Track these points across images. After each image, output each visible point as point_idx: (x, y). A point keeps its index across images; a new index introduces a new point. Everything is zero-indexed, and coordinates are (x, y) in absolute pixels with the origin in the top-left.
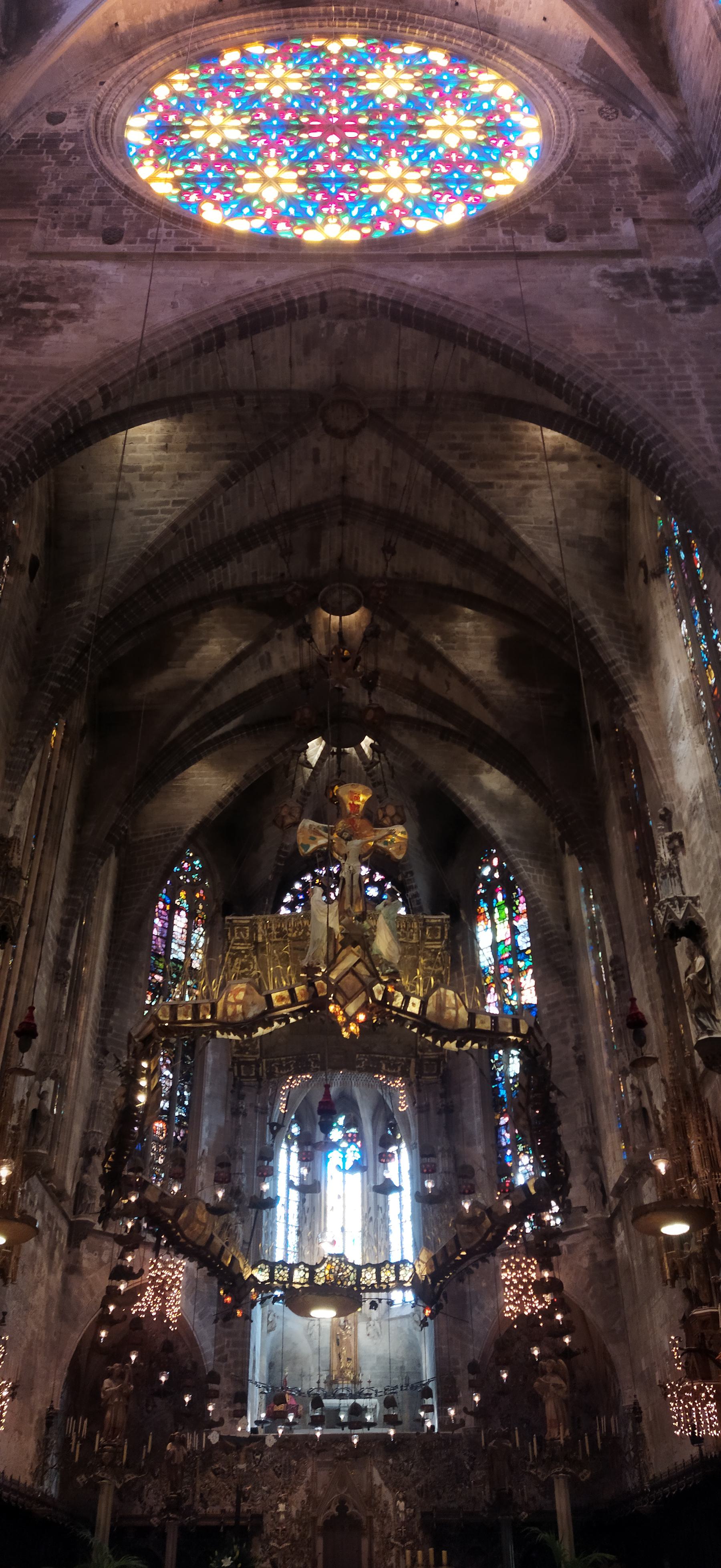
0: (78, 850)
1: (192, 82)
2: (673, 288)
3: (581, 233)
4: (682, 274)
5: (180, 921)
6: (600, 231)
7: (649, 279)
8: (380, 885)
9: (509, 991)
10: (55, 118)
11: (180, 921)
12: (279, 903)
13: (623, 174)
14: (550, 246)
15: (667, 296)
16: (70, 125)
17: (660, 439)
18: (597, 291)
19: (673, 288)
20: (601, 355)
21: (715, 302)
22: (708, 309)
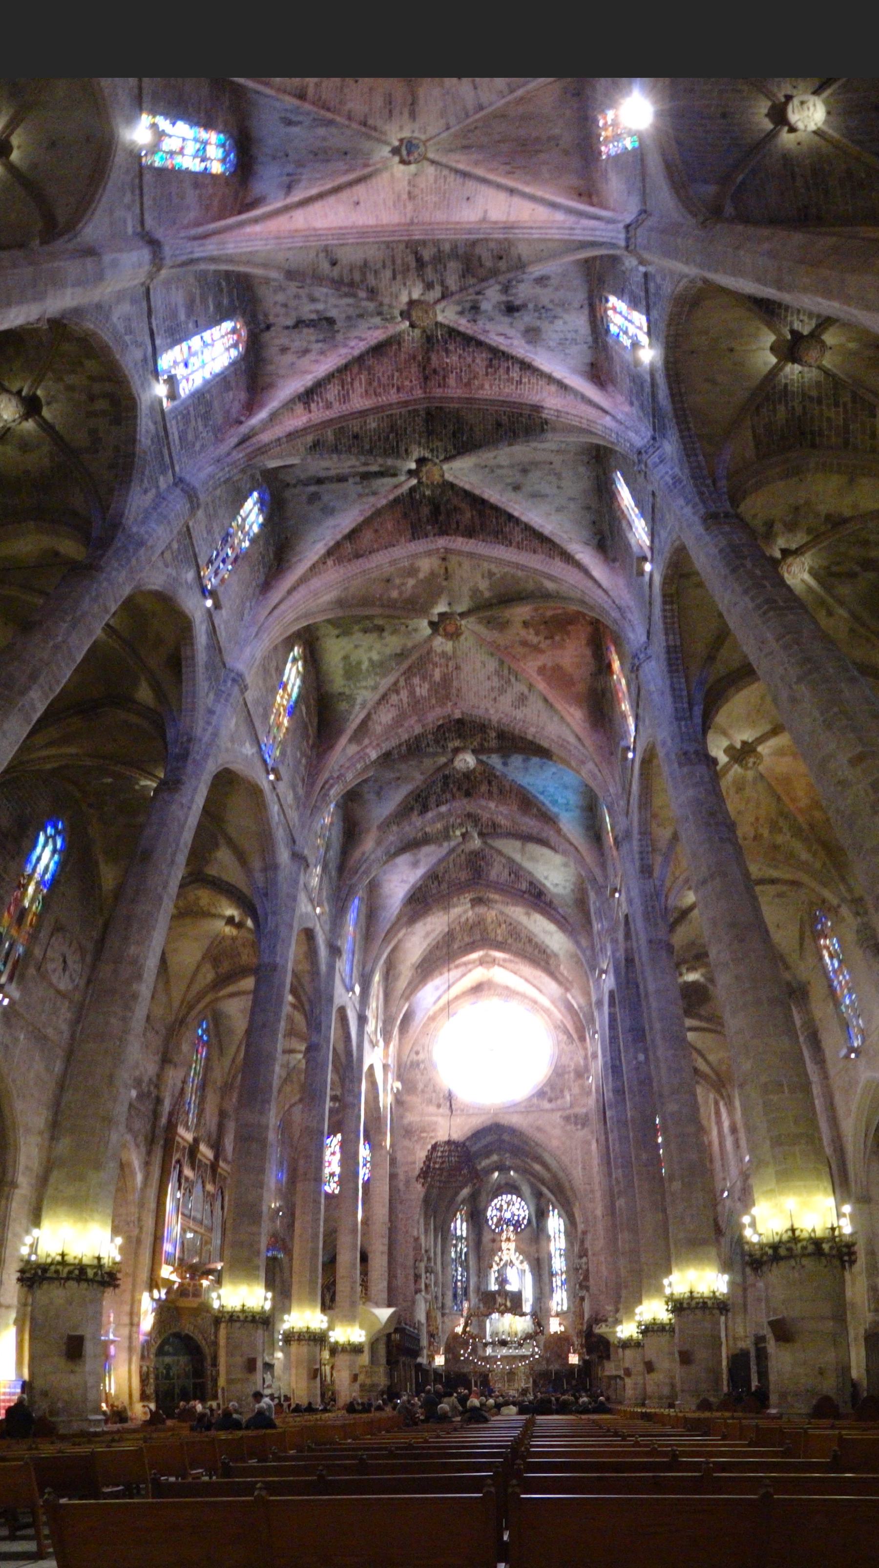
16: (421, 1056)
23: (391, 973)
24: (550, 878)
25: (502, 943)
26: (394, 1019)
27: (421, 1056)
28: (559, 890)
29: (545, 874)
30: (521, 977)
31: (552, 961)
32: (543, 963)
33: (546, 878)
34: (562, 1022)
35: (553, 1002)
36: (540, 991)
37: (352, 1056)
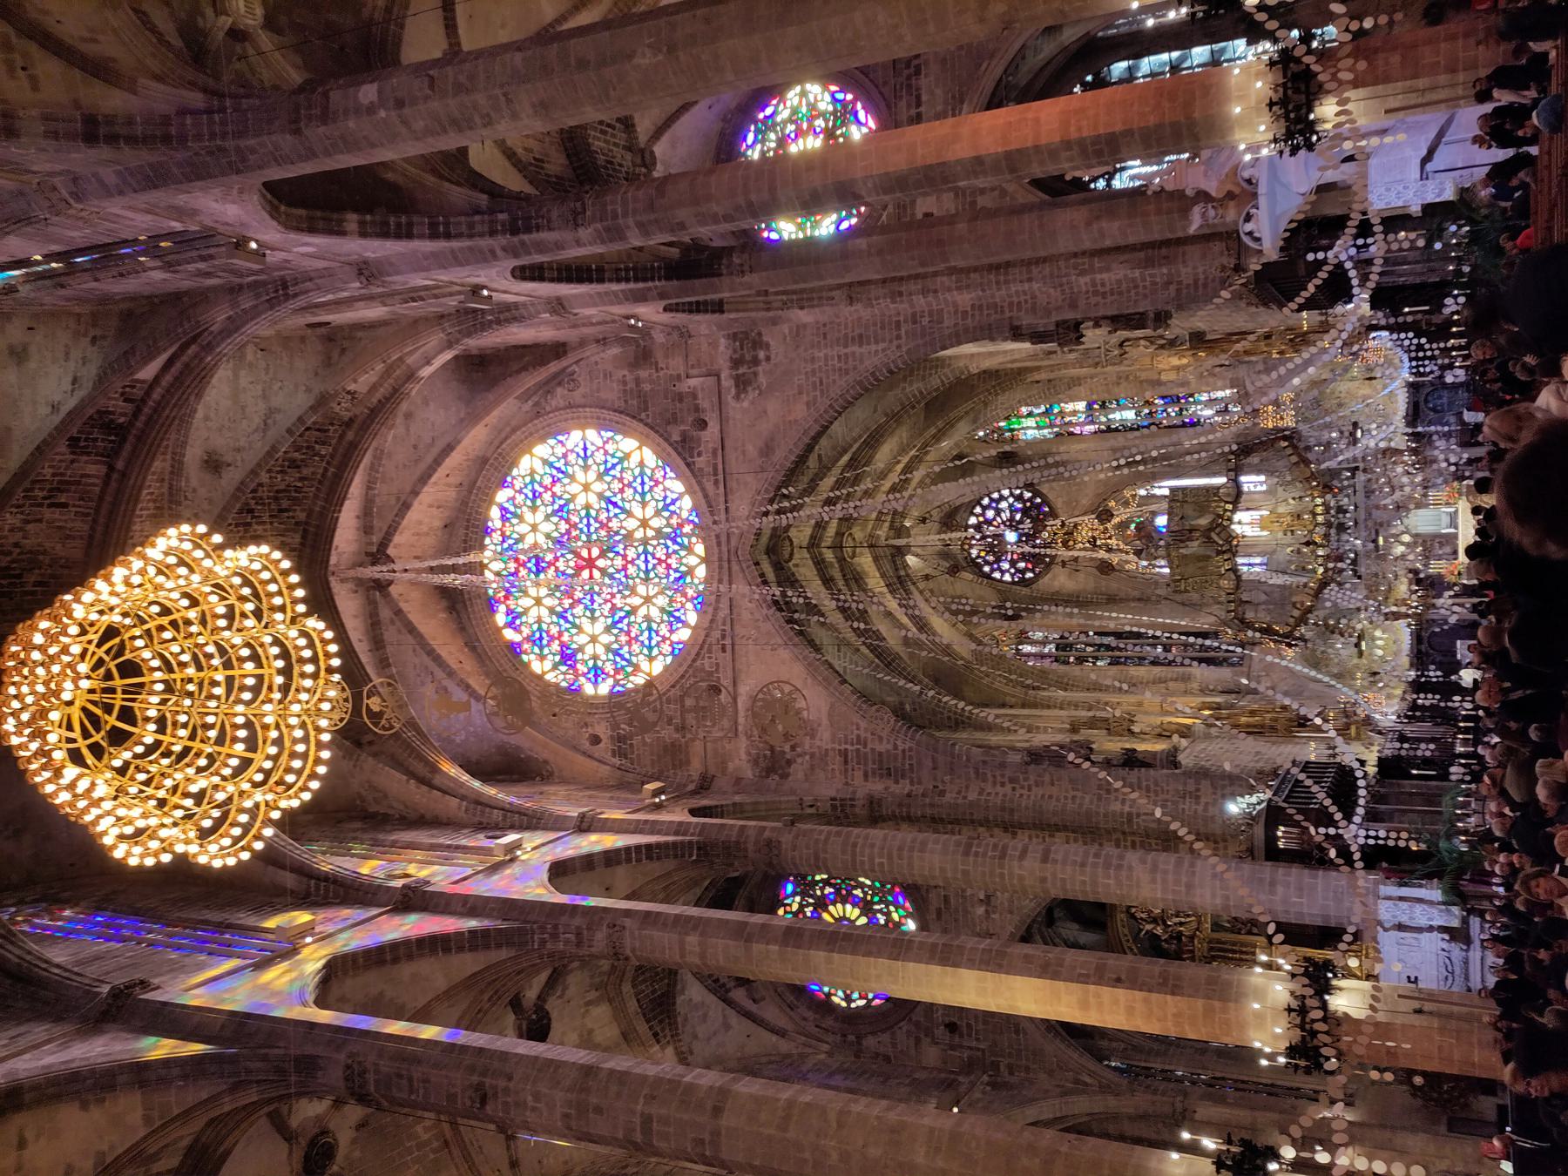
0: (1023, 706)
1: (542, 658)
2: (748, 357)
3: (697, 409)
4: (735, 351)
5: (1027, 648)
6: (695, 396)
7: (741, 371)
8: (984, 508)
9: (1074, 419)
10: (596, 740)
11: (1027, 648)
12: (1000, 581)
13: (638, 381)
14: (713, 428)
15: (755, 362)
16: (602, 730)
17: (873, 374)
18: (752, 403)
19: (748, 357)
20: (808, 404)
21: (760, 334)
22: (765, 339)
23: (373, 808)
24: (57, 398)
25: (303, 537)
26: (479, 802)
27: (602, 730)
28: (90, 372)
29: (44, 410)
30: (415, 493)
31: (342, 409)
32: (350, 435)
33: (55, 408)
34: (524, 397)
35: (473, 418)
36: (449, 449)
37: (485, 933)
